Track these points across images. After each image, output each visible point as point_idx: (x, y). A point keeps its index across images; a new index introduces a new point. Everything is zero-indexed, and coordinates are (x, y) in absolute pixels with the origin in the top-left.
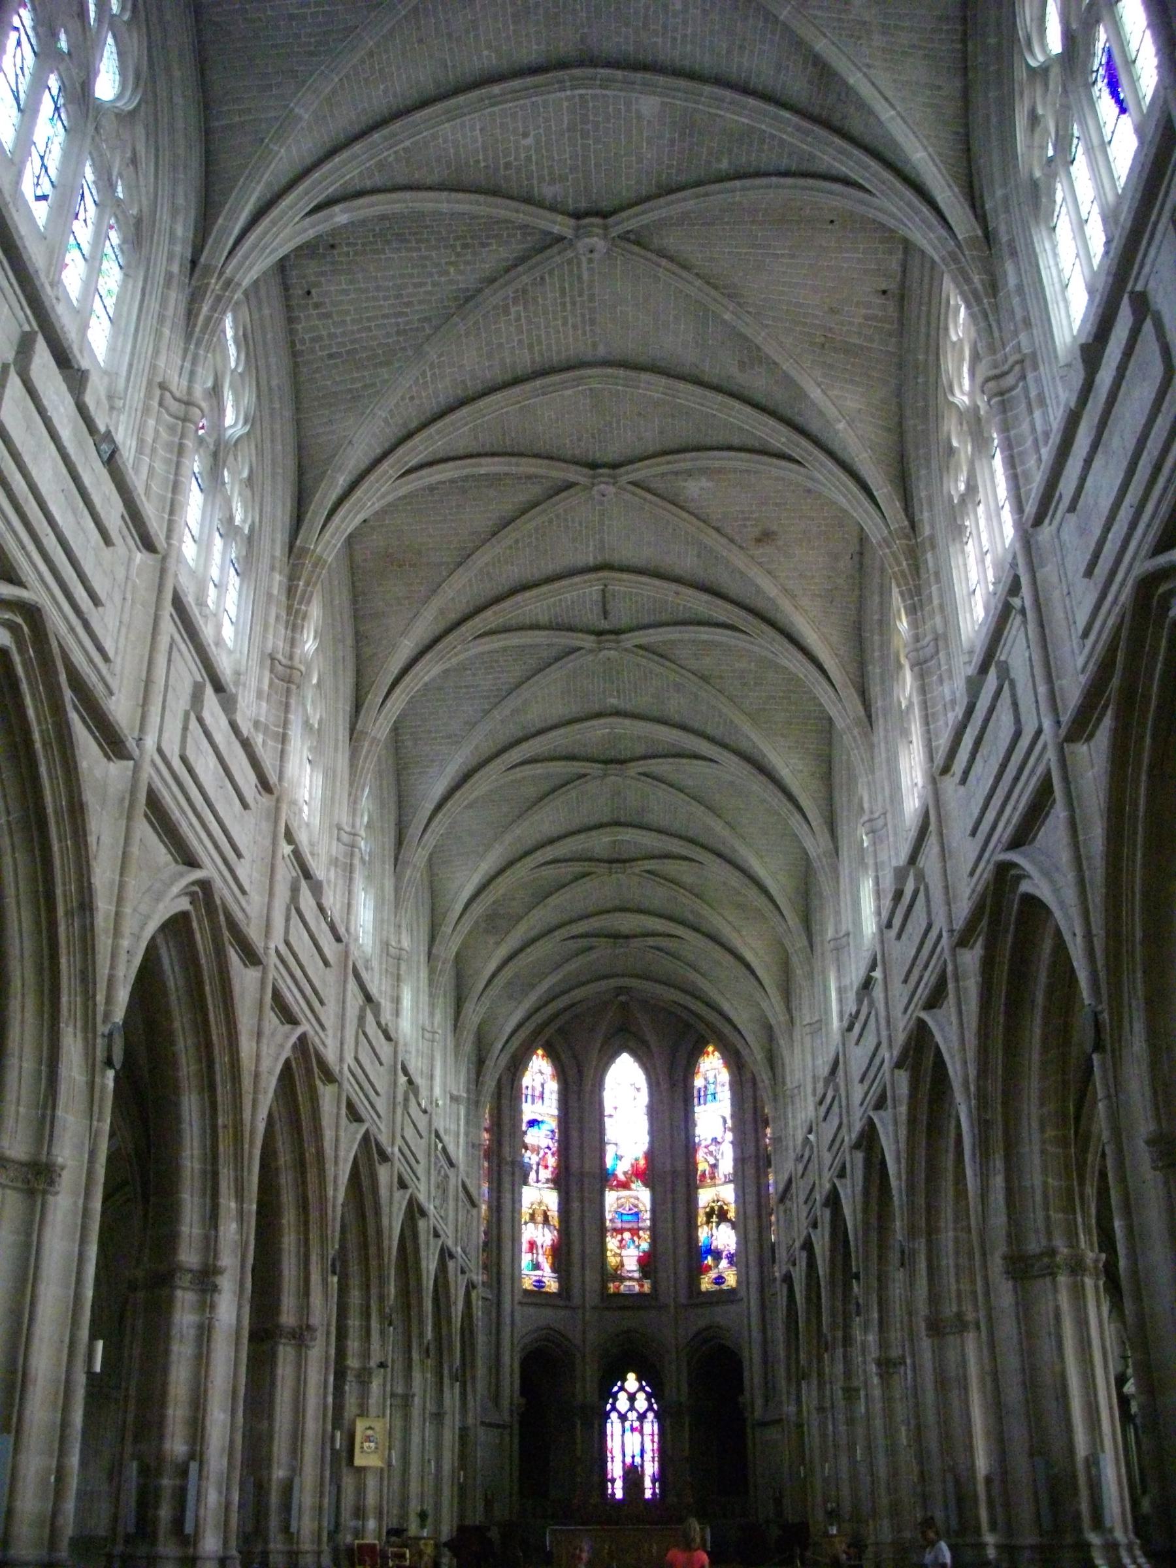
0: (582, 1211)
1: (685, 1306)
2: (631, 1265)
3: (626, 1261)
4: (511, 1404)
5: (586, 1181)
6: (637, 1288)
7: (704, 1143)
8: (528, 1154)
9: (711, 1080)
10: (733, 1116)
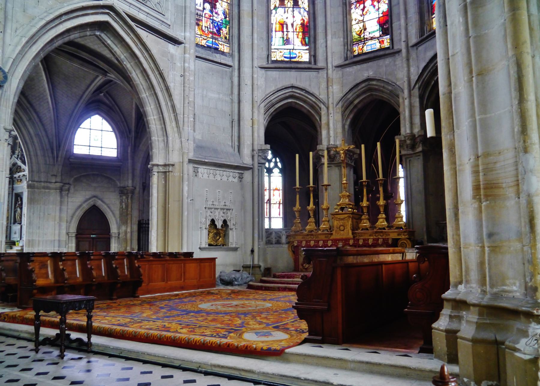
1: (417, 45)
2: (373, 28)
3: (368, 25)
4: (253, 150)
6: (378, 46)
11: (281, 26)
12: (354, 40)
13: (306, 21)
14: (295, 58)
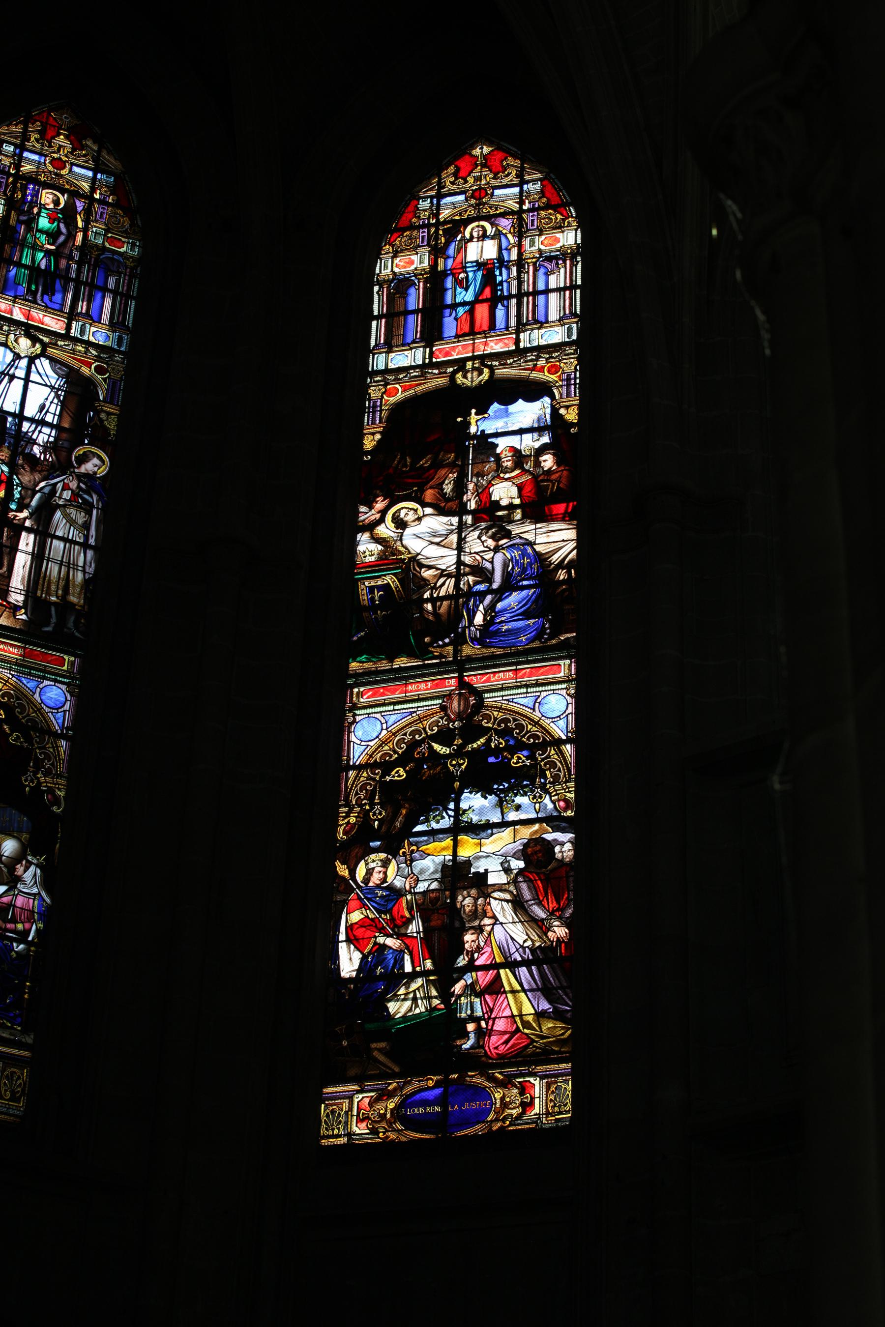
9: (44, 223)
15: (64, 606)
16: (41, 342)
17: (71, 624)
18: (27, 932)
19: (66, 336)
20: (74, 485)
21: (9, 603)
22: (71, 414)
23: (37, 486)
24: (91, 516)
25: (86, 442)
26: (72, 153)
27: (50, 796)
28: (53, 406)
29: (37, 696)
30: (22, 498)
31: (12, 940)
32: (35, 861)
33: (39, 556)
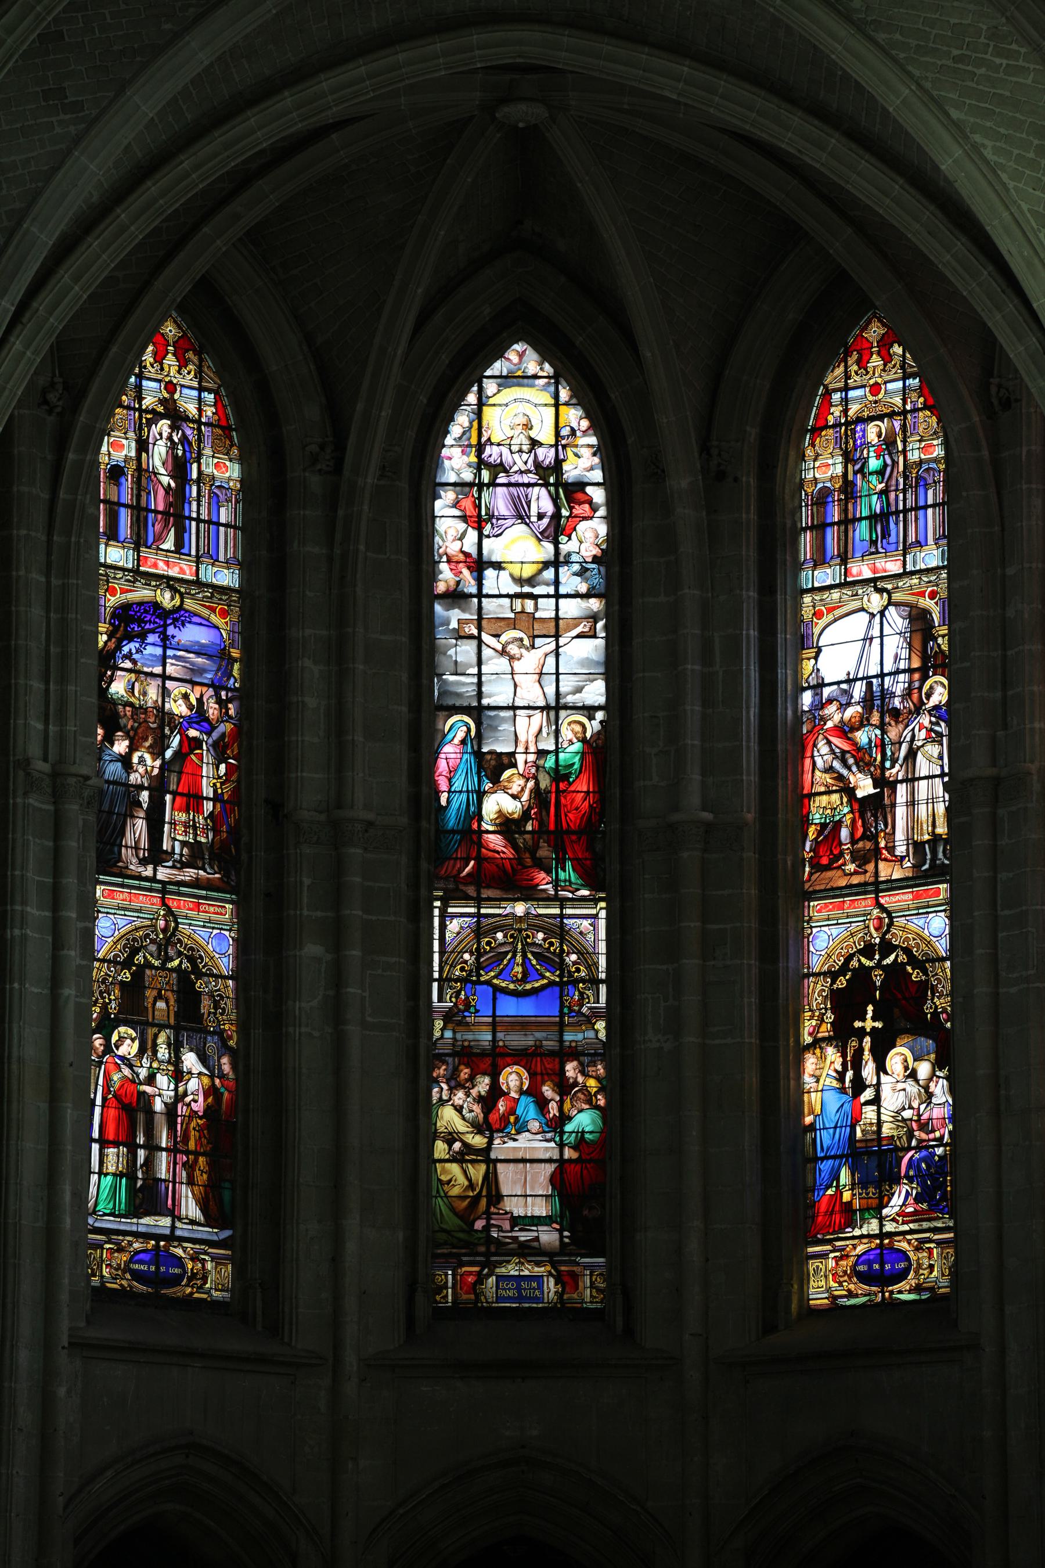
0: (337, 977)
3: (508, 1178)
5: (355, 852)
7: (834, 715)
8: (121, 747)
9: (874, 464)
10: (953, 608)
11: (124, 1115)
12: (442, 1237)
13: (226, 1095)
14: (176, 1280)
15: (936, 838)
16: (885, 590)
17: (941, 855)
18: (942, 1137)
19: (905, 574)
20: (926, 723)
21: (896, 856)
22: (918, 653)
23: (901, 737)
24: (942, 745)
25: (931, 674)
26: (884, 370)
27: (944, 1015)
28: (904, 650)
29: (926, 931)
30: (893, 754)
31: (933, 1147)
32: (941, 1074)
33: (912, 803)
